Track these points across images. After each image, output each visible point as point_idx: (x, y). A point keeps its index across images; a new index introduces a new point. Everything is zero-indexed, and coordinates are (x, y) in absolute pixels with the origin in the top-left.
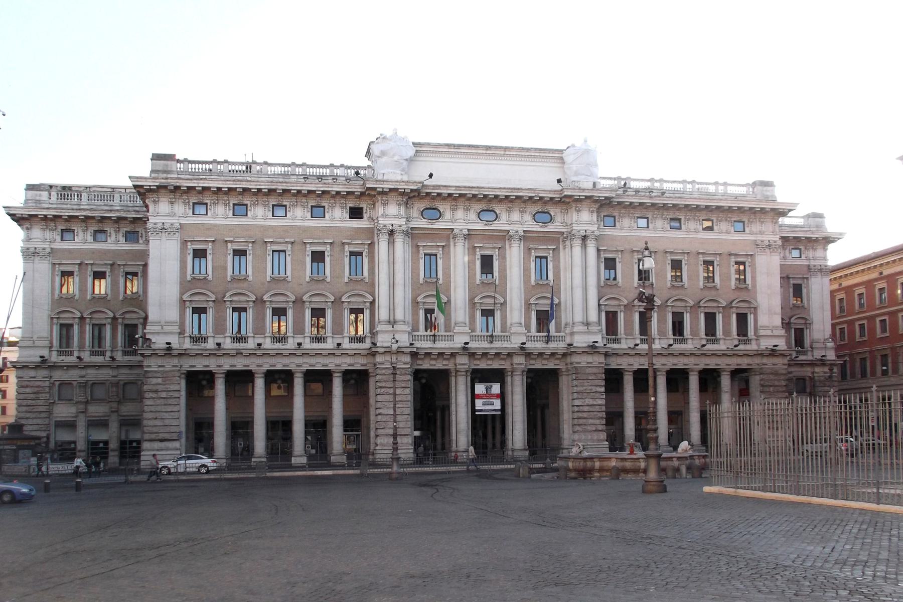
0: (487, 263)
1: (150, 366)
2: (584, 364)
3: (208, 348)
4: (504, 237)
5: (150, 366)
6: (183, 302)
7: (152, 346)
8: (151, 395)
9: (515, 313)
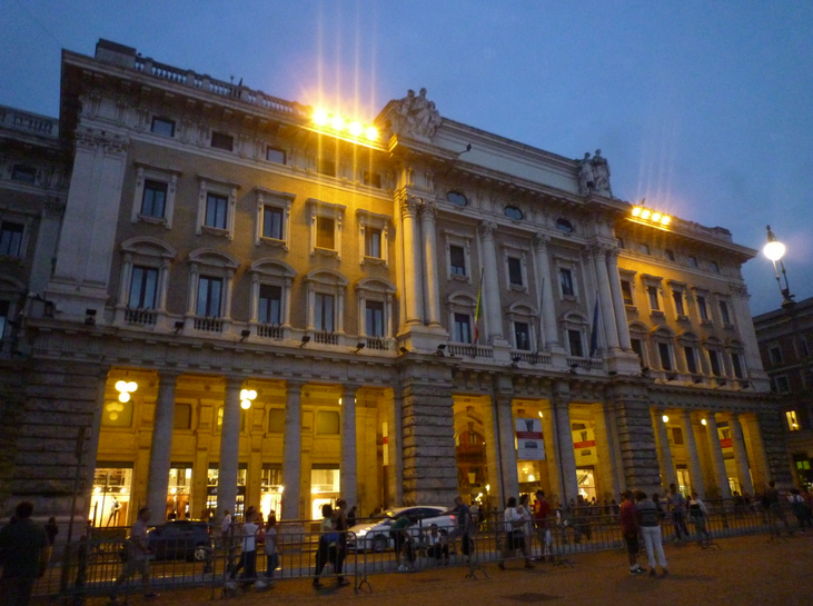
0: (515, 266)
1: (45, 352)
2: (630, 398)
3: (155, 331)
4: (532, 239)
5: (45, 352)
6: (120, 254)
7: (56, 317)
8: (39, 404)
9: (549, 332)
